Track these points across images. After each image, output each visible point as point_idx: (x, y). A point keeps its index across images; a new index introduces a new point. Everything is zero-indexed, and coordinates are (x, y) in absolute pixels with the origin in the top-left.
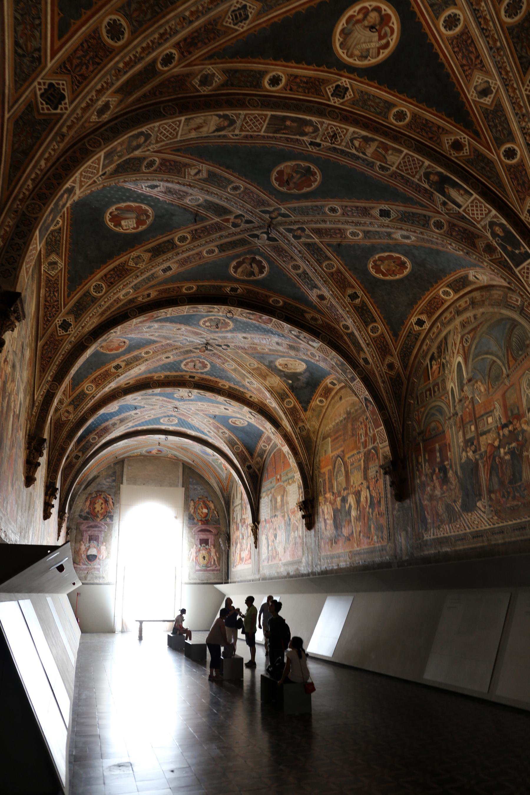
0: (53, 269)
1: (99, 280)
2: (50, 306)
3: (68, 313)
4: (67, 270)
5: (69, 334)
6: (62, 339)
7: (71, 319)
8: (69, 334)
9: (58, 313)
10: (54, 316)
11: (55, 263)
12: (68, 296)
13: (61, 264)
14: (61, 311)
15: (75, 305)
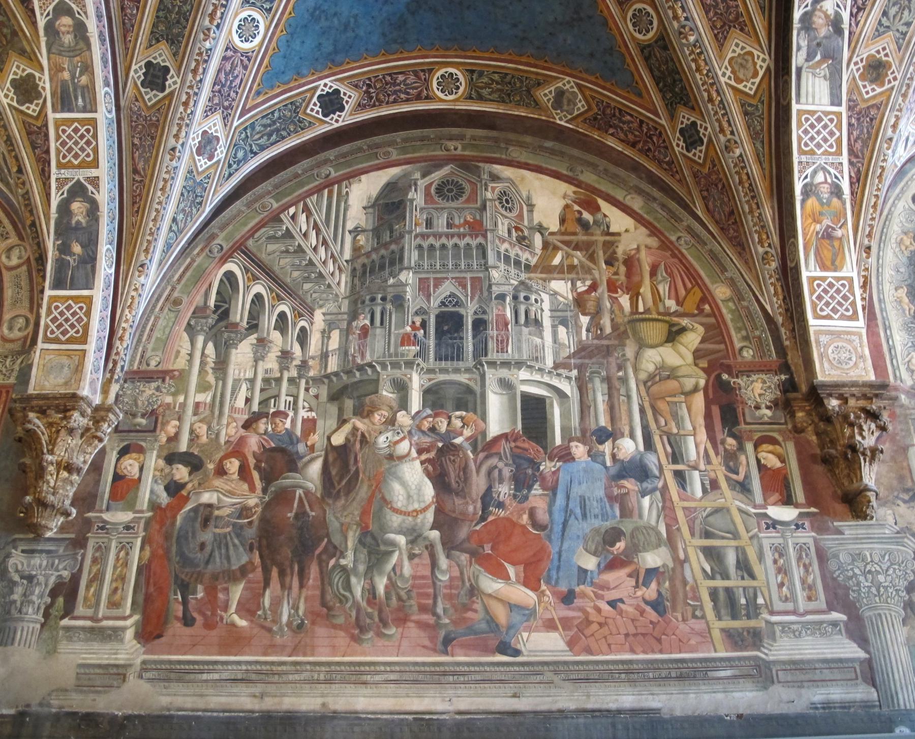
0: (572, 102)
1: (624, 12)
2: (646, 142)
3: (672, 117)
4: (585, 76)
5: (710, 140)
6: (713, 162)
7: (685, 117)
8: (710, 140)
9: (664, 135)
10: (667, 147)
11: (560, 94)
12: (640, 95)
13: (567, 83)
14: (663, 126)
15: (661, 91)
